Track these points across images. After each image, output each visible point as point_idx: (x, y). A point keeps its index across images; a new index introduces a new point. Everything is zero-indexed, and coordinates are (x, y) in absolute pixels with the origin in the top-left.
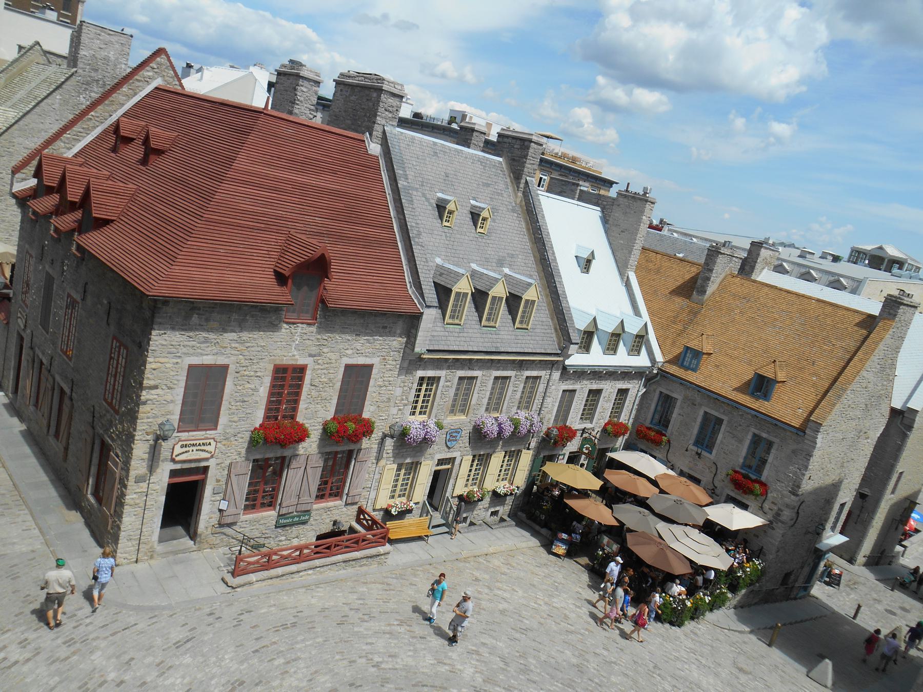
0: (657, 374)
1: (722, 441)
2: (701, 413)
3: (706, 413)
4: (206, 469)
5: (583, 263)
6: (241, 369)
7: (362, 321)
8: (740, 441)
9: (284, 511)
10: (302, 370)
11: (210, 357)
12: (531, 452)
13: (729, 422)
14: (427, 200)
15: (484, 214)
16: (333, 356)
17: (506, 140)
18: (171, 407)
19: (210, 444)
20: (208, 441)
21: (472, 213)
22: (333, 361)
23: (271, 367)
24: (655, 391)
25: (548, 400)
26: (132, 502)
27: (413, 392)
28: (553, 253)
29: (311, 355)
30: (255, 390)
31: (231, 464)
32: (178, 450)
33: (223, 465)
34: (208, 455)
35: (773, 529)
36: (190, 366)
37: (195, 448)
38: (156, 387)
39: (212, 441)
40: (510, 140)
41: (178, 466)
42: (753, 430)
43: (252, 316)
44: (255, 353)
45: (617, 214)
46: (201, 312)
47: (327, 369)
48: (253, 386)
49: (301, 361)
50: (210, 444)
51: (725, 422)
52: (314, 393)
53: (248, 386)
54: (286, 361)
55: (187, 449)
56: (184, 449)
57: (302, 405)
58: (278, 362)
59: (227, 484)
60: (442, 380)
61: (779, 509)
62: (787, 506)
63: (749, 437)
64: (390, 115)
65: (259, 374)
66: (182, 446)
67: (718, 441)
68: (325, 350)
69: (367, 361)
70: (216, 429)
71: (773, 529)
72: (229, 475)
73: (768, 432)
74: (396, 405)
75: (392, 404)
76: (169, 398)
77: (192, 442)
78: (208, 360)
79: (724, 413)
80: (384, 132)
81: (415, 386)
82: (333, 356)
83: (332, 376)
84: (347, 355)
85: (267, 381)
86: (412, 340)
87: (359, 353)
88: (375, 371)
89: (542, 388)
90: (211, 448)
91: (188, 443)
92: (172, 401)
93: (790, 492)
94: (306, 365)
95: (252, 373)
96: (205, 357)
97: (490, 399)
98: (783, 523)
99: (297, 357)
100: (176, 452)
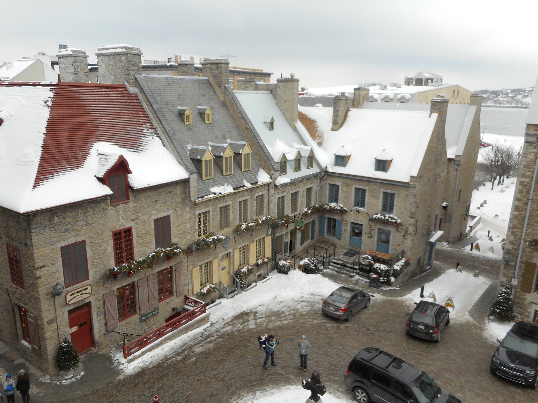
0: (325, 175)
1: (368, 202)
2: (353, 189)
3: (356, 188)
4: (89, 304)
5: (269, 125)
6: (93, 240)
7: (156, 192)
8: (377, 198)
9: (142, 312)
10: (129, 231)
11: (72, 239)
12: (270, 237)
13: (369, 190)
14: (172, 112)
15: (207, 112)
16: (145, 217)
17: (207, 66)
18: (57, 275)
19: (87, 288)
20: (86, 288)
21: (200, 113)
23: (111, 234)
24: (326, 184)
25: (272, 206)
26: (50, 337)
27: (197, 224)
28: (252, 124)
29: (132, 220)
30: (105, 250)
31: (103, 296)
32: (69, 298)
33: (99, 298)
34: (89, 295)
35: (406, 239)
36: (62, 248)
37: (79, 294)
38: (44, 266)
39: (88, 287)
40: (209, 66)
42: (383, 190)
43: (91, 208)
45: (280, 92)
47: (144, 225)
49: (128, 226)
50: (87, 288)
51: (367, 191)
52: (141, 241)
53: (100, 249)
55: (75, 296)
56: (73, 297)
58: (114, 230)
59: (104, 308)
60: (211, 212)
61: (407, 228)
62: (410, 225)
63: (381, 195)
64: (136, 68)
65: (105, 240)
67: (366, 201)
68: (140, 215)
69: (166, 214)
71: (406, 239)
72: (104, 303)
73: (391, 189)
75: (187, 234)
76: (54, 270)
77: (76, 291)
78: (72, 241)
79: (365, 186)
80: (136, 79)
81: (197, 220)
82: (145, 217)
83: (148, 229)
84: (154, 214)
85: (111, 242)
86: (188, 195)
87: (158, 210)
88: (172, 218)
89: (266, 200)
90: (89, 291)
91: (74, 292)
92: (57, 271)
93: (410, 217)
94: (131, 227)
95: (101, 241)
96: (69, 240)
97: (240, 215)
98: (410, 234)
99: (125, 223)
100: (68, 300)
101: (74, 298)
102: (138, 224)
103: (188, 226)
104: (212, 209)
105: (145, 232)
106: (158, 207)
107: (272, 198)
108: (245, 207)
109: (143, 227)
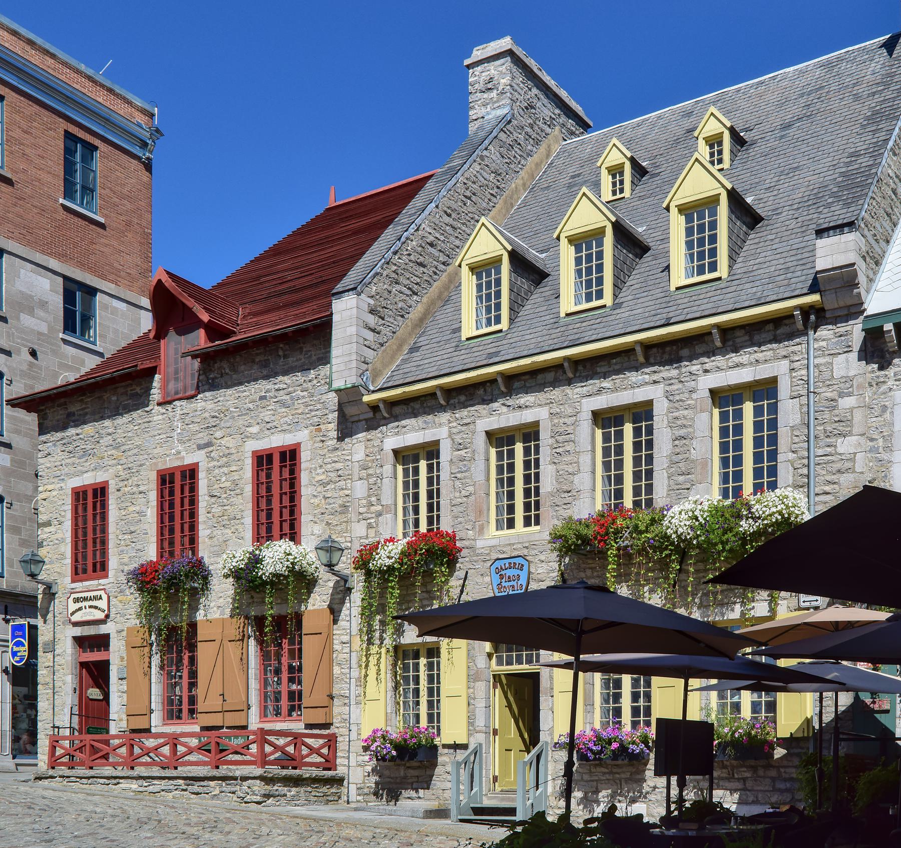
10: (191, 473)
11: (89, 474)
16: (228, 442)
19: (101, 598)
22: (233, 451)
23: (153, 476)
29: (200, 447)
30: (141, 513)
34: (100, 615)
37: (87, 604)
39: (102, 593)
41: (78, 632)
44: (131, 459)
46: (76, 417)
47: (227, 465)
48: (137, 508)
49: (189, 460)
50: (101, 598)
52: (217, 510)
53: (132, 509)
54: (171, 463)
57: (203, 532)
58: (161, 467)
65: (142, 488)
66: (77, 600)
68: (218, 434)
70: (106, 577)
74: (361, 517)
75: (353, 516)
83: (236, 476)
85: (153, 496)
88: (305, 455)
90: (103, 604)
101: (80, 609)
102: (213, 459)
103: (360, 489)
104: (451, 435)
105: (228, 484)
106: (266, 415)
107: (847, 403)
108: (645, 446)
109: (225, 470)
